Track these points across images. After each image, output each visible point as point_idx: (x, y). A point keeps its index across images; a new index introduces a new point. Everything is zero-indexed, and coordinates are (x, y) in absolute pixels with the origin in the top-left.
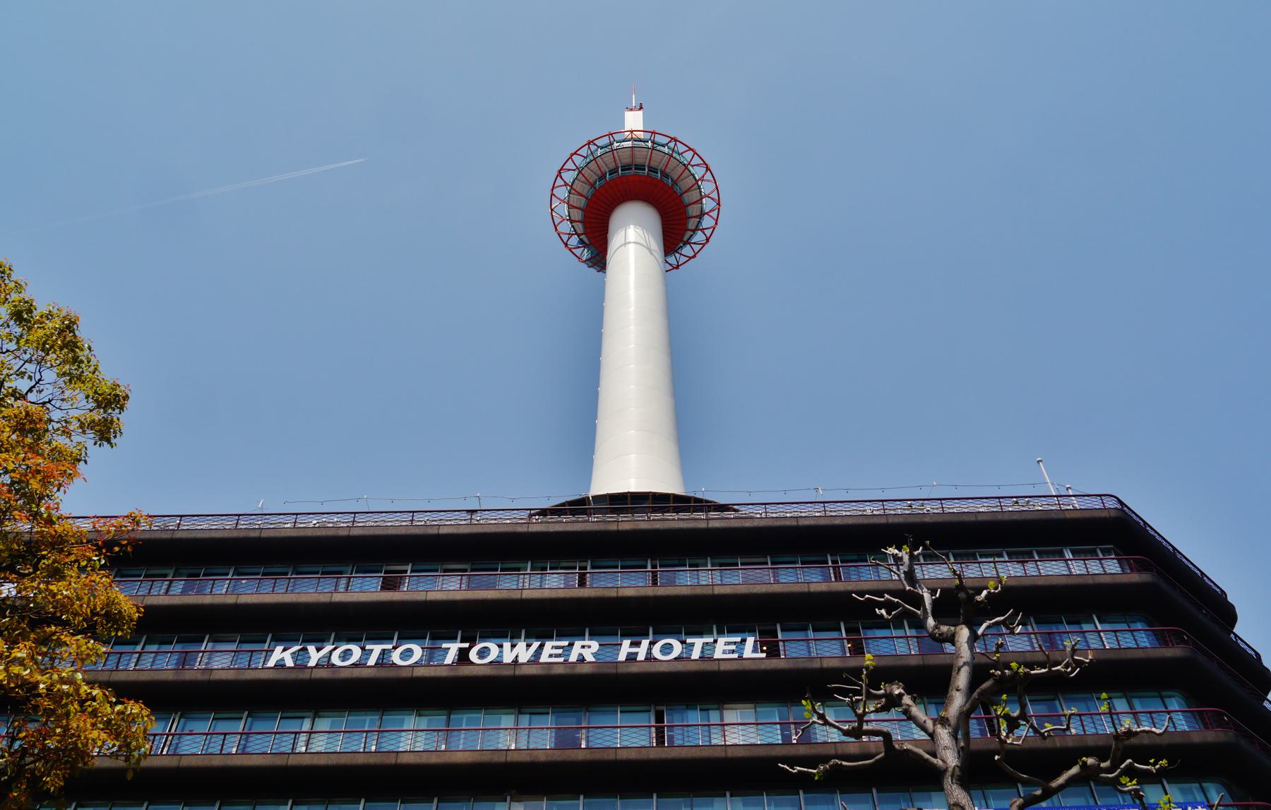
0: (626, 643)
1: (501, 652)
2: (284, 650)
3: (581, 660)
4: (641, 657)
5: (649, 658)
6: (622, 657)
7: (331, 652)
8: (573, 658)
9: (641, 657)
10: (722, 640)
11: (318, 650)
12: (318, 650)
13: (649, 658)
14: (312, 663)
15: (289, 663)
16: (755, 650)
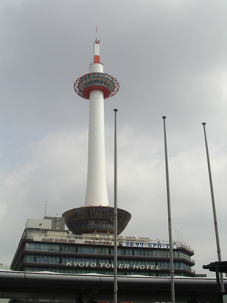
0: (135, 265)
1: (111, 265)
2: (69, 262)
3: (126, 267)
4: (137, 268)
5: (139, 268)
6: (134, 268)
7: (78, 264)
8: (125, 268)
9: (137, 268)
10: (152, 266)
11: (76, 263)
12: (76, 263)
13: (139, 268)
14: (75, 266)
15: (71, 265)
16: (158, 268)
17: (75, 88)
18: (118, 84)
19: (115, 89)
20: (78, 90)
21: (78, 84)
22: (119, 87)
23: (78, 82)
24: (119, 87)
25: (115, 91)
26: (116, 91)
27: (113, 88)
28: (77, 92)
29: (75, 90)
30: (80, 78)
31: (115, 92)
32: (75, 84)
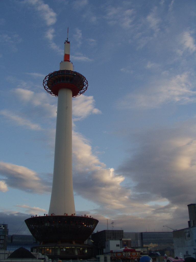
17: (45, 85)
18: (87, 82)
19: (84, 87)
20: (47, 87)
21: (46, 82)
22: (88, 85)
23: (47, 79)
24: (88, 85)
25: (84, 89)
26: (85, 90)
27: (81, 86)
28: (47, 89)
29: (45, 87)
30: (49, 75)
31: (83, 91)
32: (44, 81)
